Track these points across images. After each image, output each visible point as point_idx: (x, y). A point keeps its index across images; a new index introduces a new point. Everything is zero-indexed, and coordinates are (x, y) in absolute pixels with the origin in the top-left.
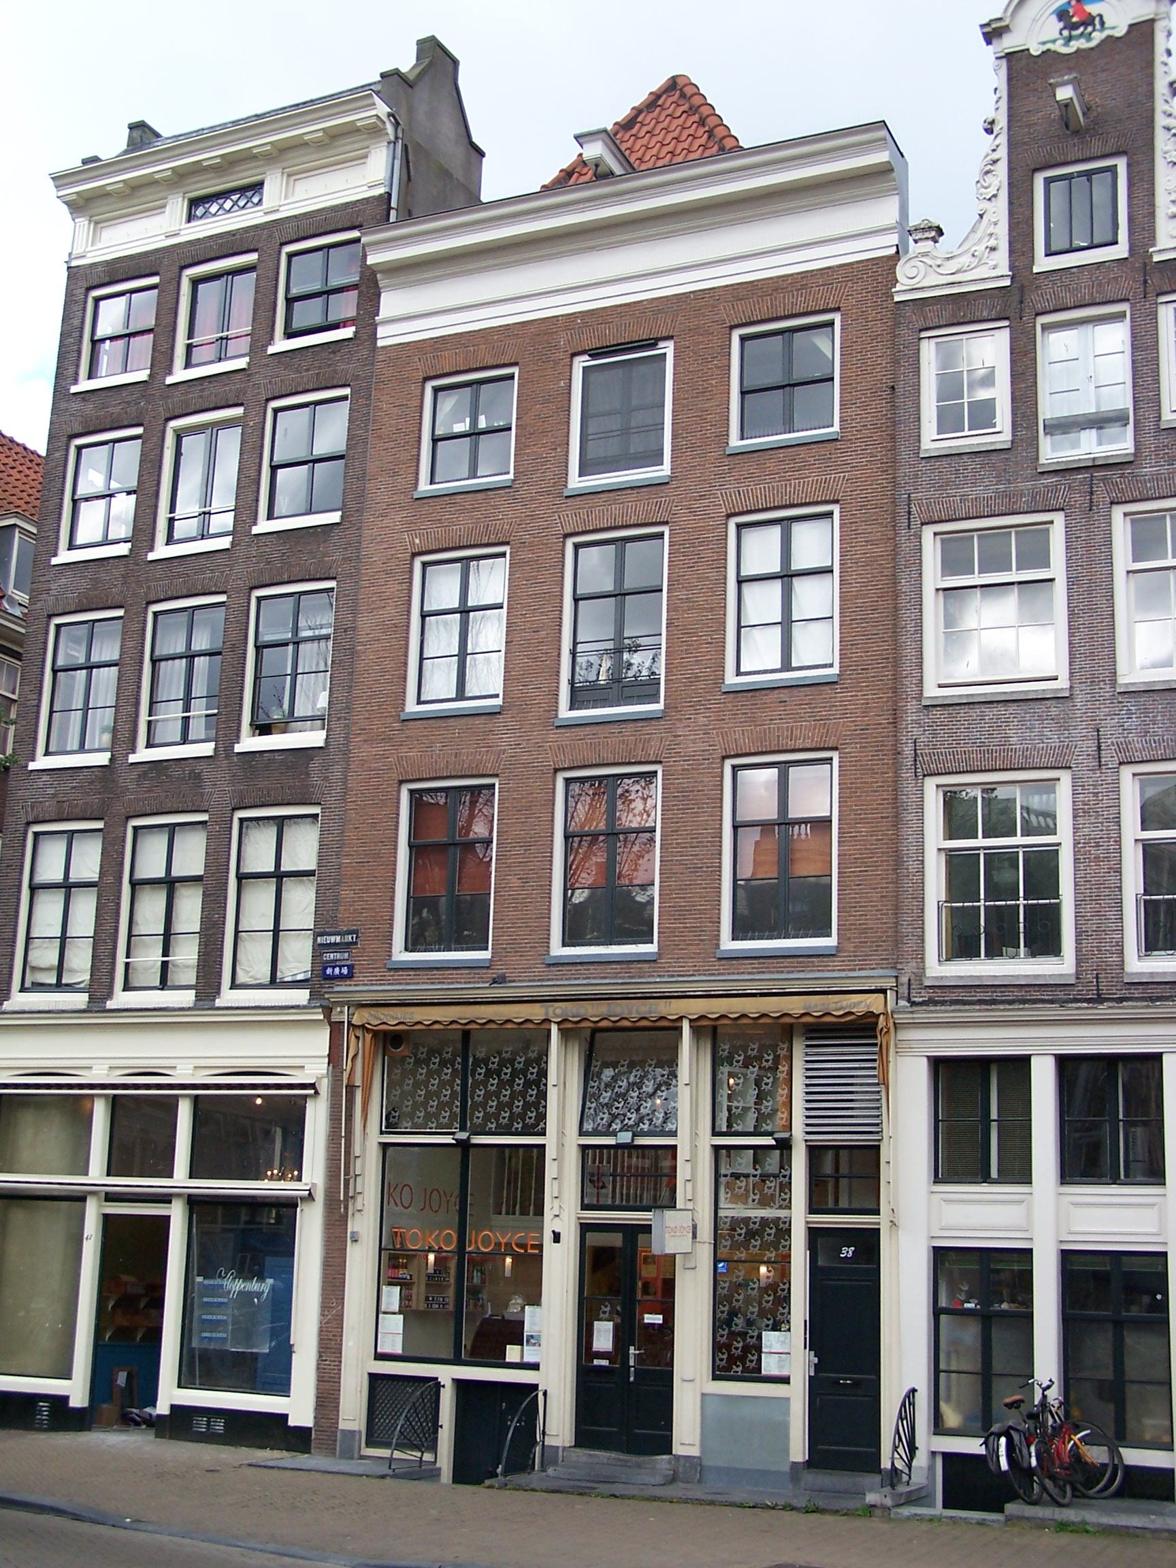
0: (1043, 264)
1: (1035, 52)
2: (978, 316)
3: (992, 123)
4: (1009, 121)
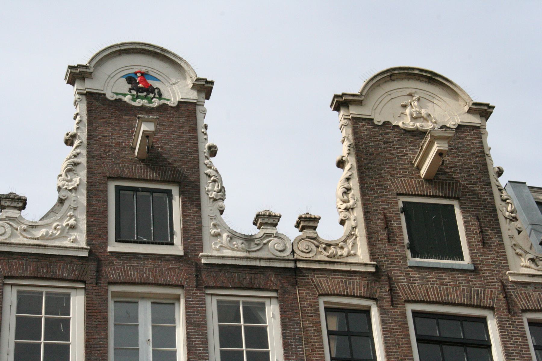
0: (114, 247)
1: (110, 96)
2: (59, 274)
3: (74, 136)
4: (88, 139)
